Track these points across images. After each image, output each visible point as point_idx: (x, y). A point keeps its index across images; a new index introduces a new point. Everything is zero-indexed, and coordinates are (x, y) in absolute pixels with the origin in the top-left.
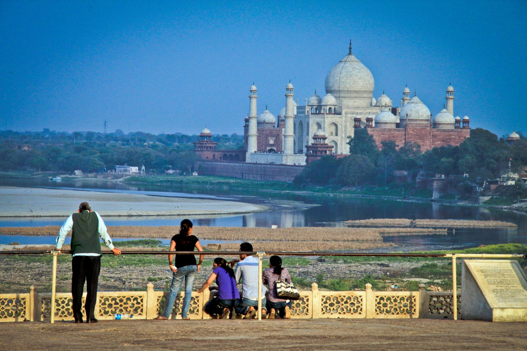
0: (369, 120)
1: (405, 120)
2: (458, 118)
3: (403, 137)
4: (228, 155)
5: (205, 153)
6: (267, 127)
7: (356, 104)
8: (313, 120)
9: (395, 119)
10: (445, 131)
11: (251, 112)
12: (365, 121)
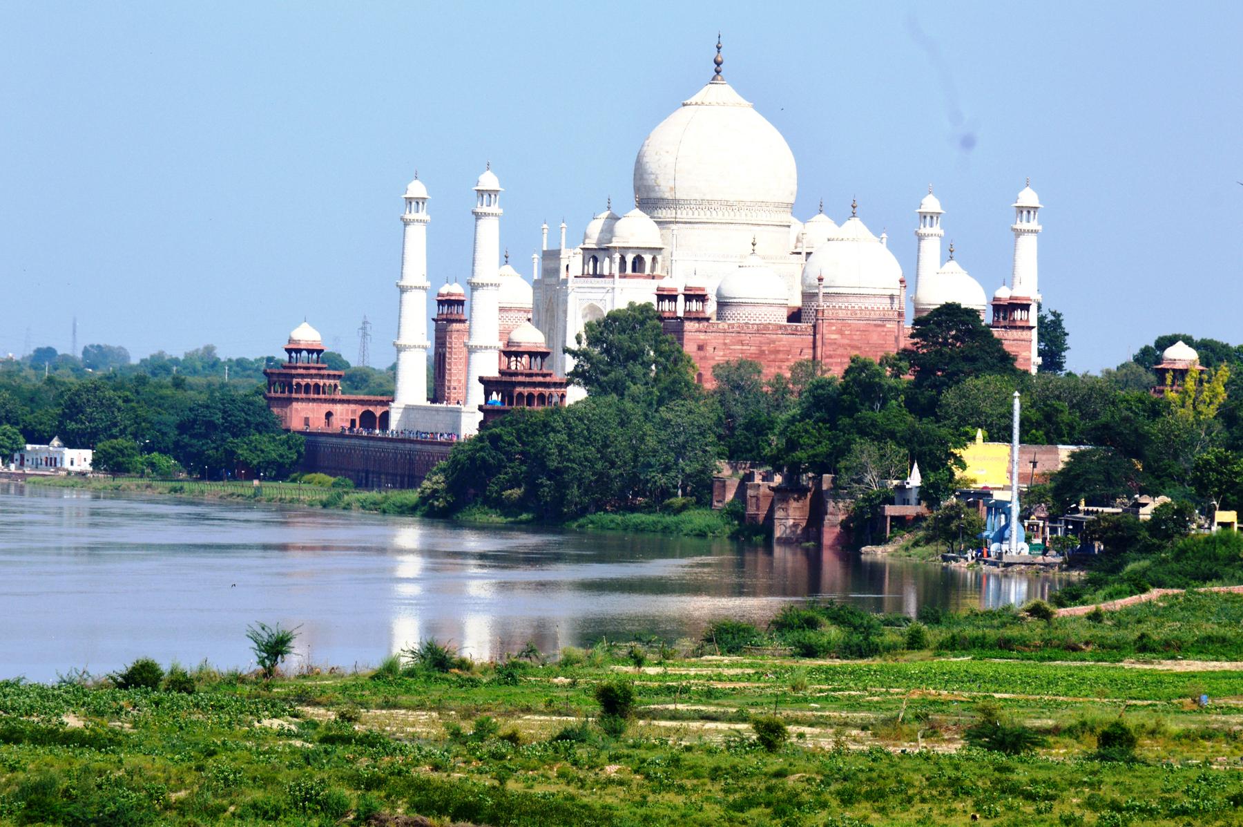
4: (378, 415)
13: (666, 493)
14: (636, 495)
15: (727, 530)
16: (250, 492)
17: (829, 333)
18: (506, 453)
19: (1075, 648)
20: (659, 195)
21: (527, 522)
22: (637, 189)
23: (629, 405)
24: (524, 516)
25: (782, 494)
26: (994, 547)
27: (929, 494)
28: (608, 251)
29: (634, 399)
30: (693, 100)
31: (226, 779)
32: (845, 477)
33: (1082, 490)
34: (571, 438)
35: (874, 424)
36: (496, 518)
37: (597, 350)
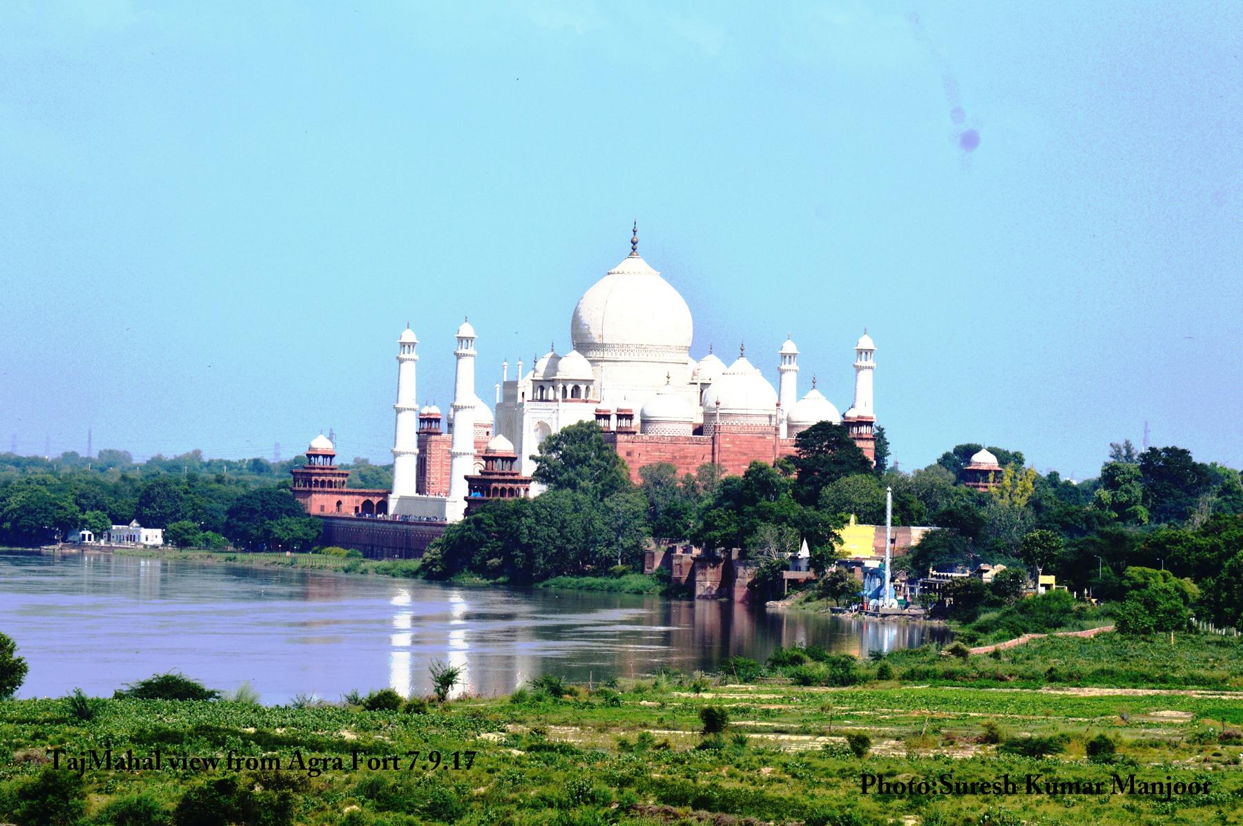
4: (375, 503)
13: (610, 561)
14: (585, 563)
15: (659, 589)
16: (288, 561)
17: (724, 443)
18: (486, 532)
19: (1002, 679)
21: (504, 583)
22: (574, 336)
23: (580, 496)
24: (501, 579)
25: (700, 563)
26: (872, 602)
27: (817, 563)
28: (553, 383)
29: (585, 491)
30: (615, 270)
31: (514, 779)
32: (753, 550)
33: (933, 560)
34: (538, 521)
35: (771, 511)
36: (477, 580)
37: (554, 456)
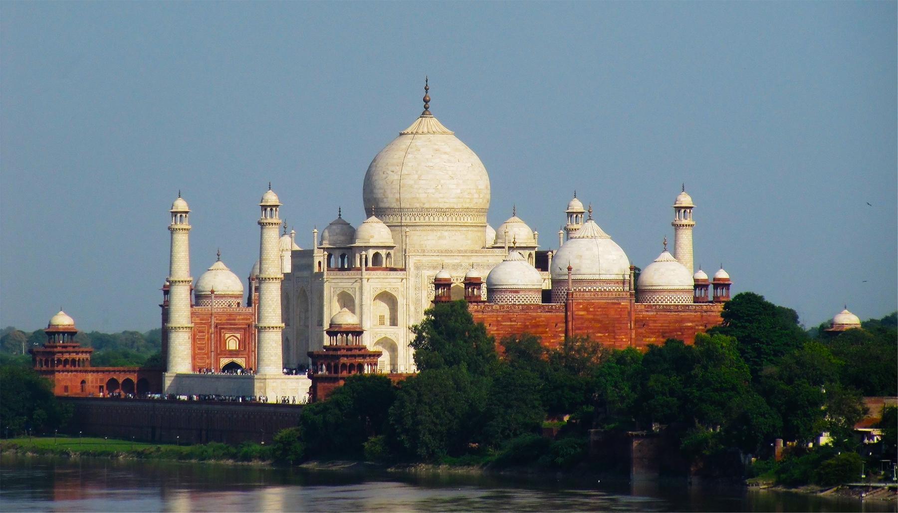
0: (471, 283)
1: (566, 282)
2: (702, 276)
3: (561, 327)
4: (120, 381)
5: (59, 376)
6: (217, 306)
7: (445, 244)
8: (332, 286)
9: (541, 280)
10: (667, 309)
11: (175, 266)
12: (463, 285)
20: (387, 205)
30: (409, 130)
